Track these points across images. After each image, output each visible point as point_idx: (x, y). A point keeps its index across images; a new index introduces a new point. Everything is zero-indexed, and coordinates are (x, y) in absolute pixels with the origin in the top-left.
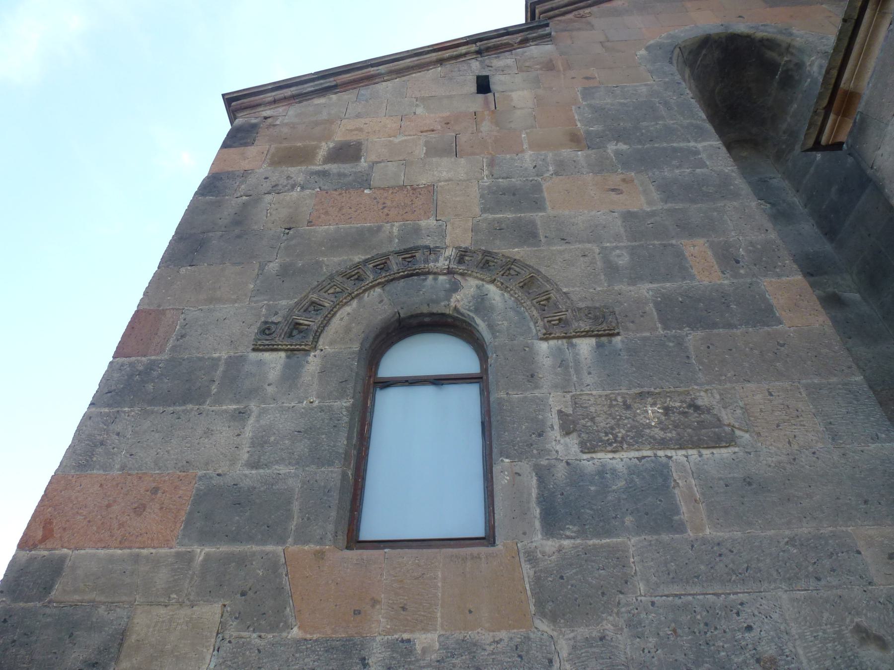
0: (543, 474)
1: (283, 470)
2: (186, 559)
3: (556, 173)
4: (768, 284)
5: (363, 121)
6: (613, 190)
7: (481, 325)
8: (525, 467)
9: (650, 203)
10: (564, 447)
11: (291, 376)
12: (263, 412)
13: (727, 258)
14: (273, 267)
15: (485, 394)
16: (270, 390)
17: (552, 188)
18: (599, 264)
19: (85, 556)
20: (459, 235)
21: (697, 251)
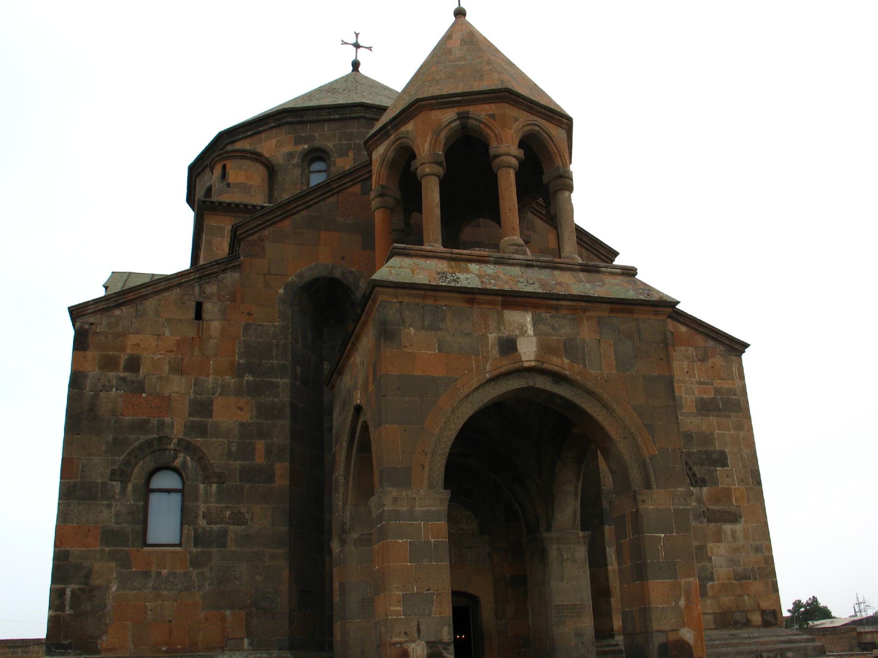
0: (195, 530)
1: (125, 525)
2: (103, 551)
3: (220, 394)
4: (277, 465)
5: (141, 336)
6: (240, 408)
7: (184, 475)
8: (191, 528)
9: (251, 418)
10: (202, 522)
11: (124, 490)
12: (116, 505)
13: (269, 451)
14: (110, 438)
15: (183, 496)
16: (117, 497)
17: (219, 403)
18: (226, 450)
19: (75, 550)
20: (178, 431)
21: (260, 445)
